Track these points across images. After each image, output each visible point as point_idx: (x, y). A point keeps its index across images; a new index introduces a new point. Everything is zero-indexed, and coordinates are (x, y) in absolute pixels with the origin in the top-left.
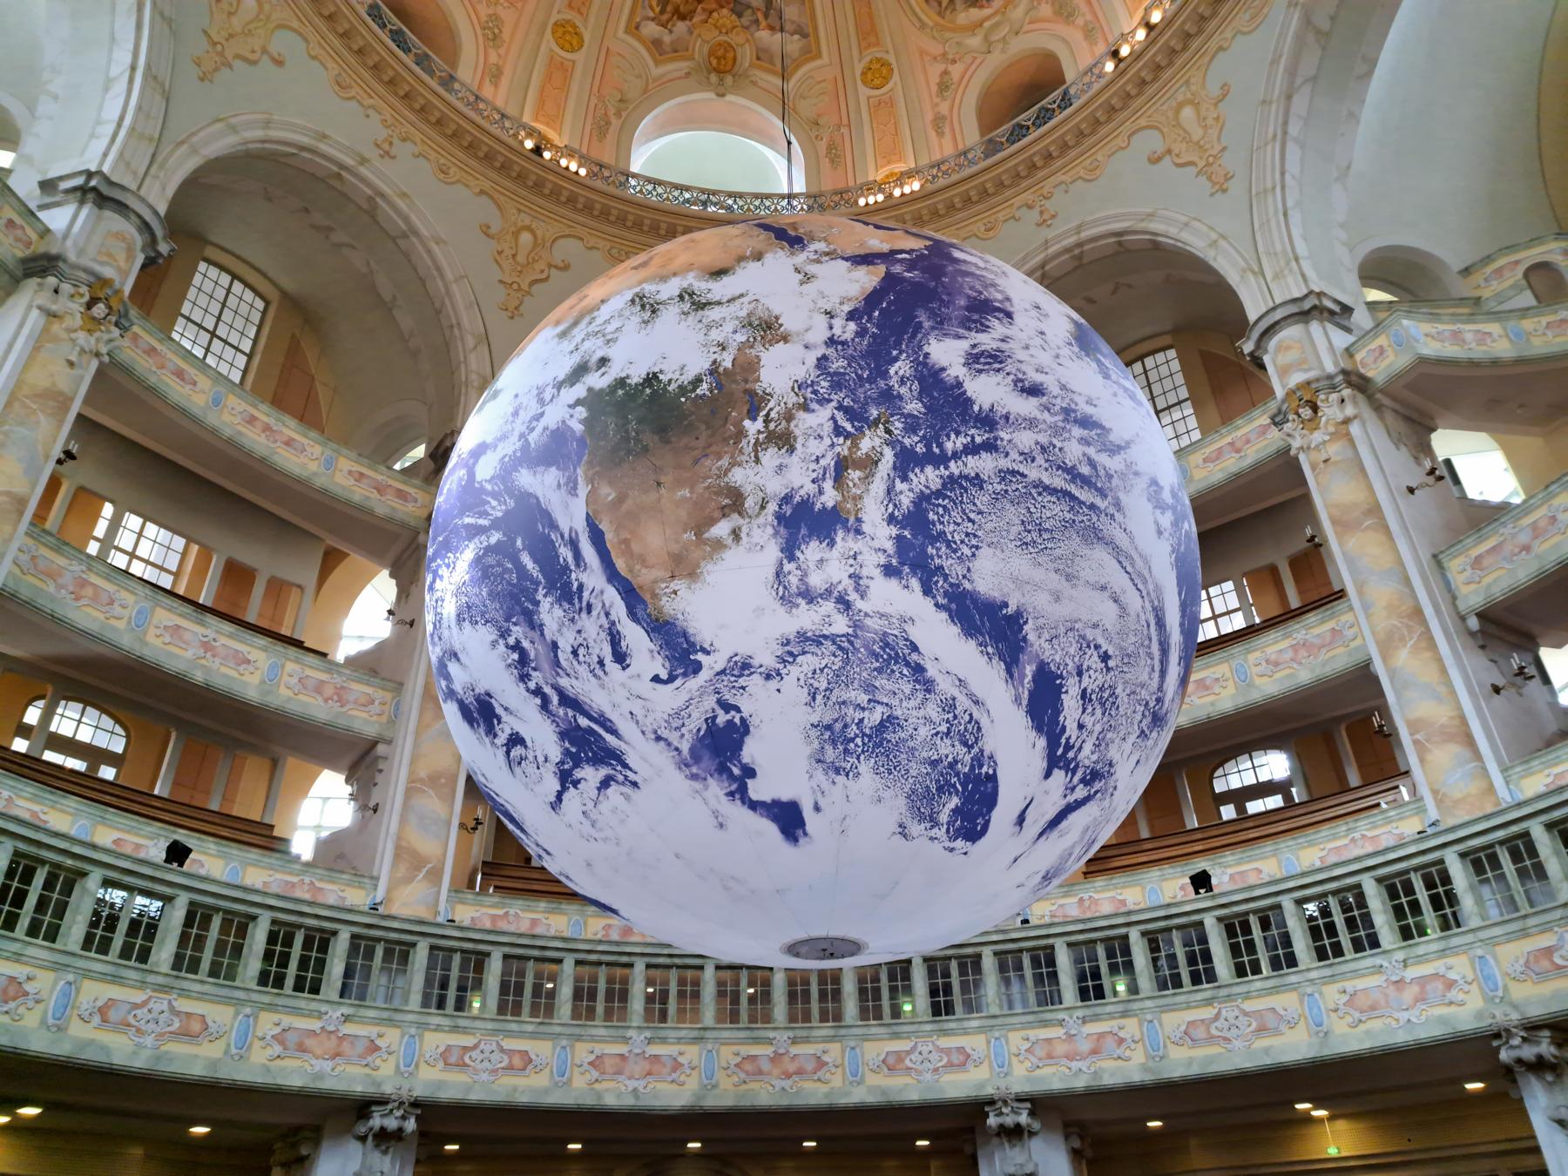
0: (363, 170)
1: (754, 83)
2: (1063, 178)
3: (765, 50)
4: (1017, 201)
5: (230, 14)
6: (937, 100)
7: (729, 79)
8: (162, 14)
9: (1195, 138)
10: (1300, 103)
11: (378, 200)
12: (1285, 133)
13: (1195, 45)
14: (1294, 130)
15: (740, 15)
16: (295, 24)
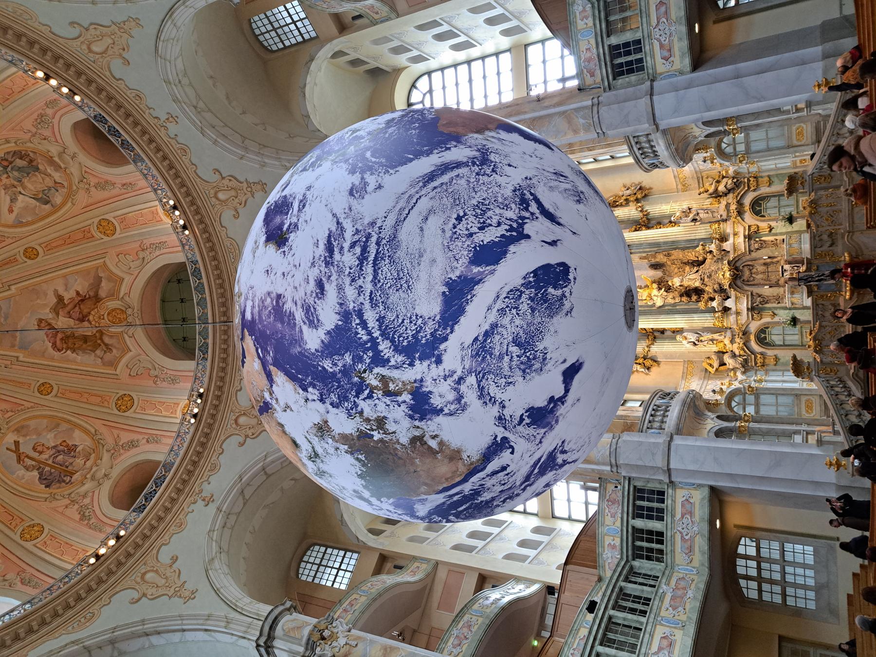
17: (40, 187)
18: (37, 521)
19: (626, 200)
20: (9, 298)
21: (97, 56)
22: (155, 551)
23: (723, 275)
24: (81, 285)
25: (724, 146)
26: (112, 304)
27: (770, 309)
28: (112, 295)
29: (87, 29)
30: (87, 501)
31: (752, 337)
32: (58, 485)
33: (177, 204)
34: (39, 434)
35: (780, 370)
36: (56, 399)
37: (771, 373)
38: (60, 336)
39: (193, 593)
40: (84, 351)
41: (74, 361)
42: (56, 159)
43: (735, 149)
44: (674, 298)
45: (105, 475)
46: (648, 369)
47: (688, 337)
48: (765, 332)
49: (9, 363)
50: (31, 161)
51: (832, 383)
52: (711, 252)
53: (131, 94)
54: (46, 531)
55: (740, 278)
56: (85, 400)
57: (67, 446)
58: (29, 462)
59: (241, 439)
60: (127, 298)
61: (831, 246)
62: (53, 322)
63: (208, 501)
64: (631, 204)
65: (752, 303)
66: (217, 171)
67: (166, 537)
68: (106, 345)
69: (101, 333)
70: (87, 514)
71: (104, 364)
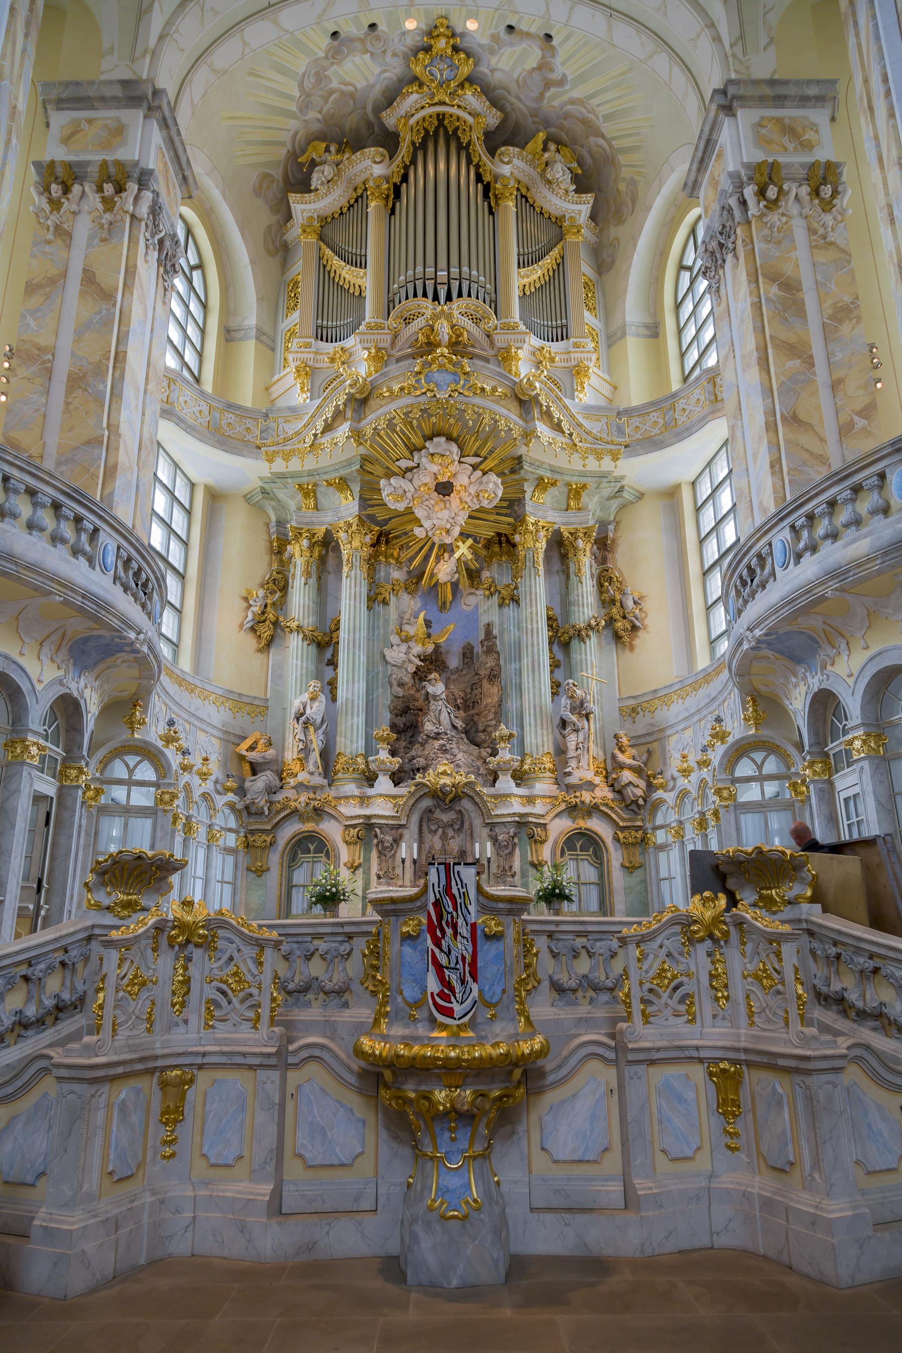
19: (613, 602)
23: (444, 773)
25: (758, 756)
27: (367, 860)
31: (309, 826)
35: (235, 878)
37: (230, 859)
43: (748, 779)
44: (401, 685)
46: (253, 629)
47: (316, 704)
48: (319, 850)
51: (53, 984)
52: (494, 754)
55: (439, 806)
61: (558, 988)
64: (604, 611)
65: (381, 826)
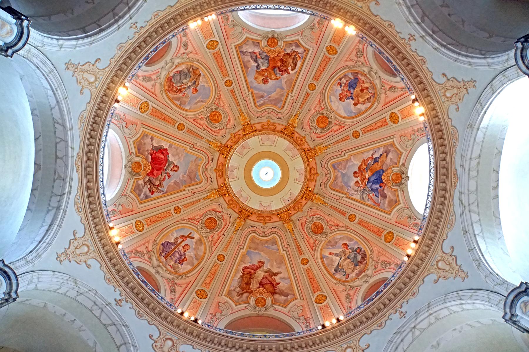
0: (424, 34)
1: (260, 35)
2: (131, 41)
3: (257, 46)
4: (148, 27)
5: (457, 94)
6: (188, 40)
7: (270, 36)
8: (481, 105)
9: (86, 73)
10: (53, 102)
11: (420, 21)
12: (53, 91)
13: (99, 100)
14: (50, 92)
15: (266, 56)
16: (434, 83)
17: (345, 268)
18: (145, 231)
20: (278, 249)
21: (436, 266)
22: (99, 260)
24: (283, 285)
26: (269, 301)
28: (275, 301)
29: (451, 255)
30: (146, 257)
32: (161, 249)
33: (341, 322)
34: (194, 249)
36: (213, 262)
38: (252, 271)
39: (61, 261)
40: (241, 282)
41: (235, 276)
42: (364, 274)
45: (158, 272)
49: (241, 244)
50: (361, 262)
53: (415, 289)
54: (138, 232)
56: (209, 275)
57: (183, 260)
58: (180, 240)
59: (155, 337)
60: (272, 309)
62: (262, 269)
63: (118, 302)
66: (369, 346)
67: (105, 270)
68: (242, 294)
69: (251, 292)
70: (138, 254)
71: (229, 291)
